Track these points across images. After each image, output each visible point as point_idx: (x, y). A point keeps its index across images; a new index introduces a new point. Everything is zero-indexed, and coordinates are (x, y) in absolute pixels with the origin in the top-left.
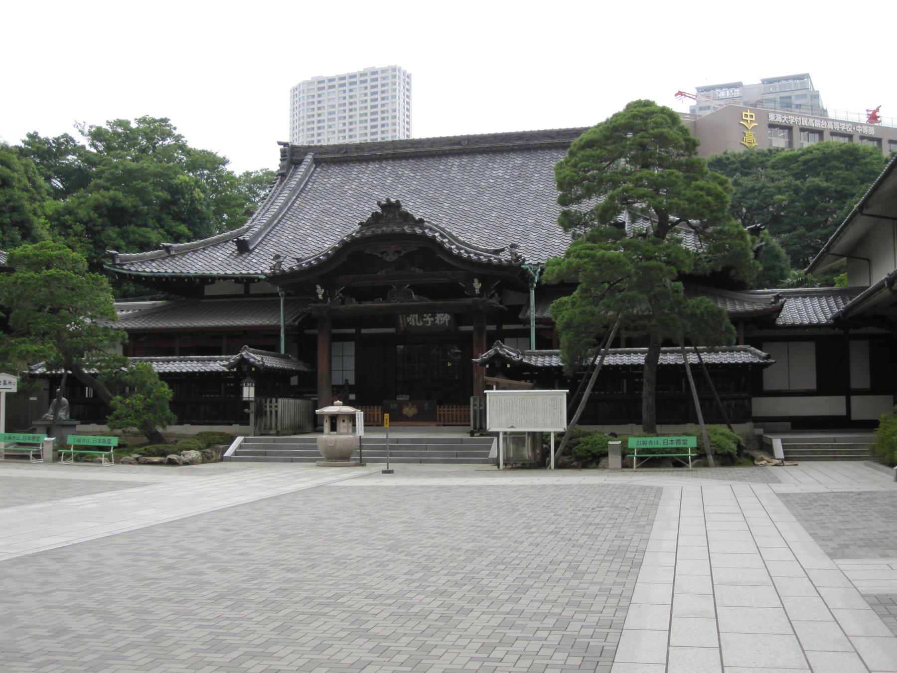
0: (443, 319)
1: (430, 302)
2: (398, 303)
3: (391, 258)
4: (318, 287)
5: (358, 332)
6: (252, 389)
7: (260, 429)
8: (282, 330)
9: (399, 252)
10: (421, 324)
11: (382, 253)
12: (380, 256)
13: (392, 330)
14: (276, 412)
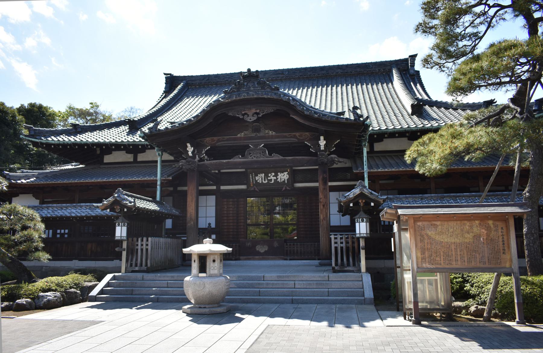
0: (283, 177)
1: (281, 158)
2: (255, 159)
4: (189, 145)
5: (218, 188)
6: (125, 229)
7: (131, 265)
8: (159, 183)
9: (257, 114)
10: (266, 181)
11: (243, 115)
12: (241, 117)
13: (244, 187)
14: (147, 250)
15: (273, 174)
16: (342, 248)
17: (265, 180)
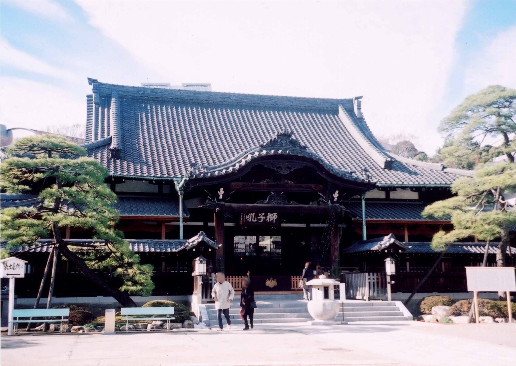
0: (273, 217)
2: (276, 205)
3: (285, 172)
9: (290, 168)
10: (256, 220)
12: (276, 170)
15: (264, 214)
16: (374, 283)
17: (254, 219)
